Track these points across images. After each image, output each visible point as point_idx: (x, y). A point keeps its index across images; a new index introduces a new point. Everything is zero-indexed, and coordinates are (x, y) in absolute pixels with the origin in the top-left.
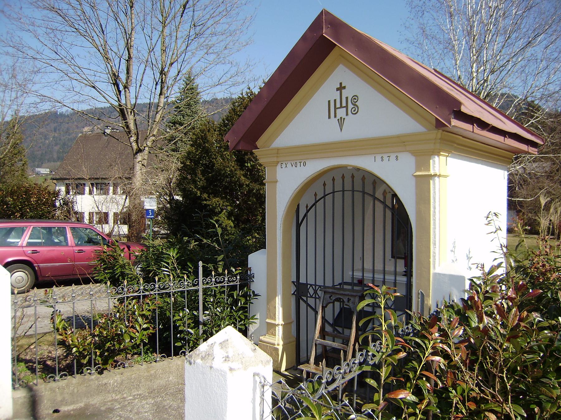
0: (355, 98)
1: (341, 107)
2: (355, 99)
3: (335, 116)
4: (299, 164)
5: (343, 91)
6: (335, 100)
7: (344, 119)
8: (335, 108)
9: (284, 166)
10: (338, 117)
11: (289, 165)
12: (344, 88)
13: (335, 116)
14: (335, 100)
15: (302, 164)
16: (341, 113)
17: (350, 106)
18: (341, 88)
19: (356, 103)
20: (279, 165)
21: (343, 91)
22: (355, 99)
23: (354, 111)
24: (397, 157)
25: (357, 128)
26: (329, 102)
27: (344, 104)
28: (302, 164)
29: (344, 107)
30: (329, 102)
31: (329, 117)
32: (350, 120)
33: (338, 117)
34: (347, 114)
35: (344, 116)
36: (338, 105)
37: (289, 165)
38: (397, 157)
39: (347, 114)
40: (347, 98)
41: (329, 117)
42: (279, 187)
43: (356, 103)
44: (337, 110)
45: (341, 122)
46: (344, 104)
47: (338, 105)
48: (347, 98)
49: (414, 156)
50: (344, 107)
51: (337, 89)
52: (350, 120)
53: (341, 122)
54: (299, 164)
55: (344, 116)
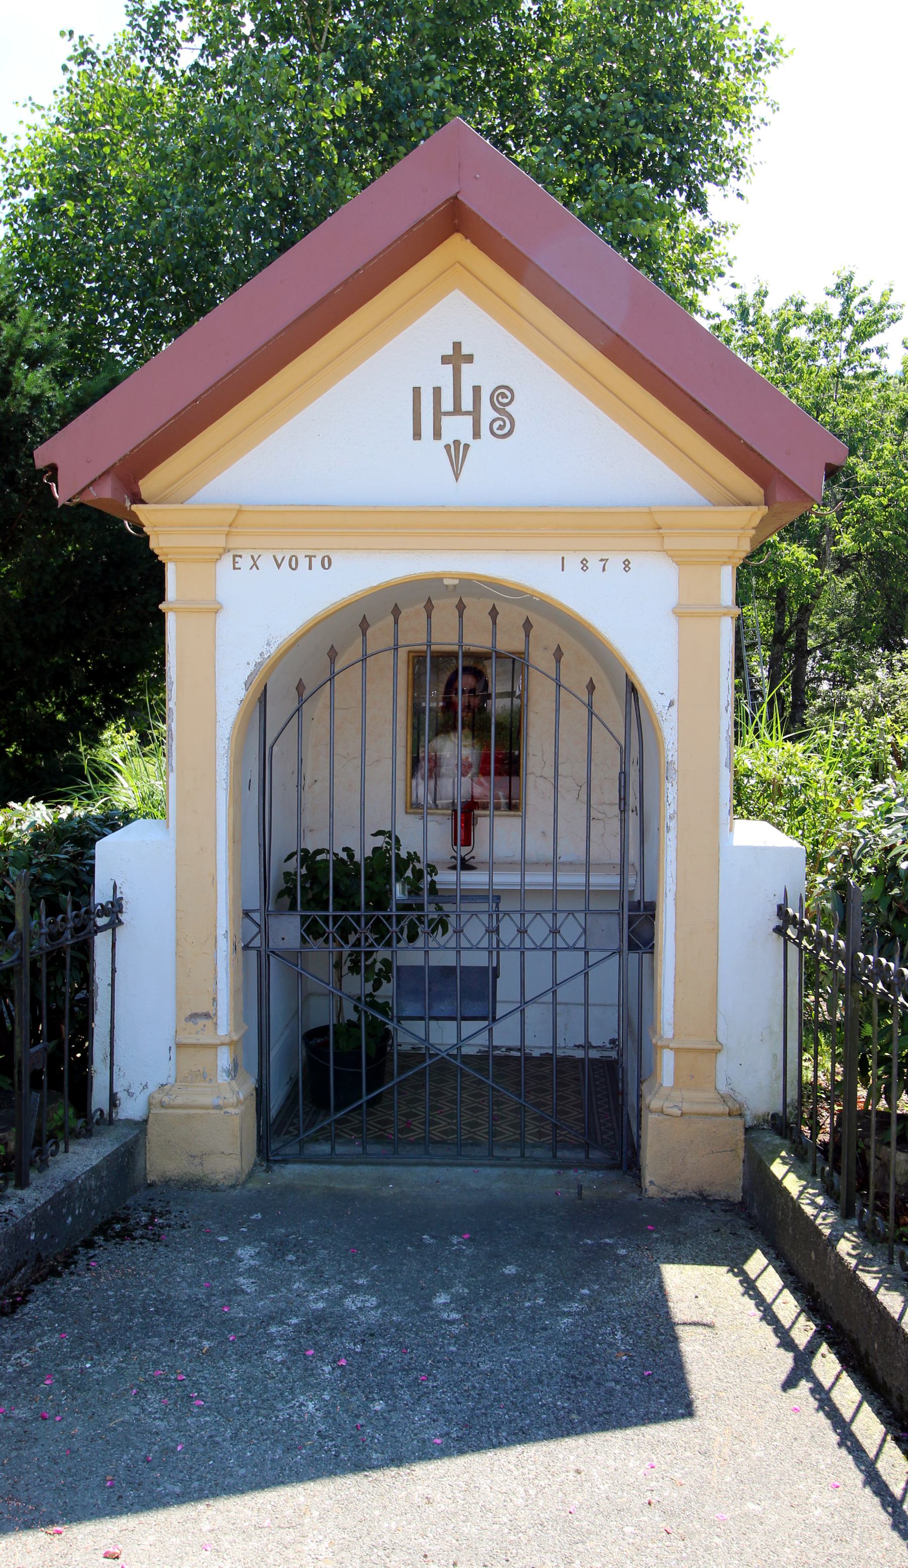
0: (503, 396)
1: (457, 410)
2: (504, 396)
3: (437, 435)
4: (304, 562)
5: (465, 367)
6: (437, 391)
7: (467, 446)
8: (438, 414)
9: (245, 562)
10: (448, 438)
11: (266, 562)
12: (469, 359)
13: (437, 435)
14: (437, 391)
15: (317, 562)
16: (457, 428)
17: (487, 413)
18: (457, 358)
19: (507, 408)
20: (228, 559)
21: (465, 367)
22: (504, 396)
23: (501, 428)
24: (627, 564)
25: (498, 472)
26: (417, 391)
27: (467, 403)
28: (317, 562)
29: (467, 413)
30: (417, 391)
31: (417, 435)
32: (484, 450)
33: (448, 438)
34: (477, 434)
35: (466, 436)
36: (447, 404)
37: (266, 562)
38: (627, 564)
39: (477, 434)
40: (477, 390)
41: (417, 435)
42: (227, 626)
43: (507, 408)
44: (446, 421)
45: (457, 454)
46: (467, 403)
47: (447, 404)
48: (477, 390)
49: (677, 563)
50: (467, 413)
51: (445, 360)
52: (484, 450)
53: (457, 454)
54: (304, 562)
55: (466, 436)
